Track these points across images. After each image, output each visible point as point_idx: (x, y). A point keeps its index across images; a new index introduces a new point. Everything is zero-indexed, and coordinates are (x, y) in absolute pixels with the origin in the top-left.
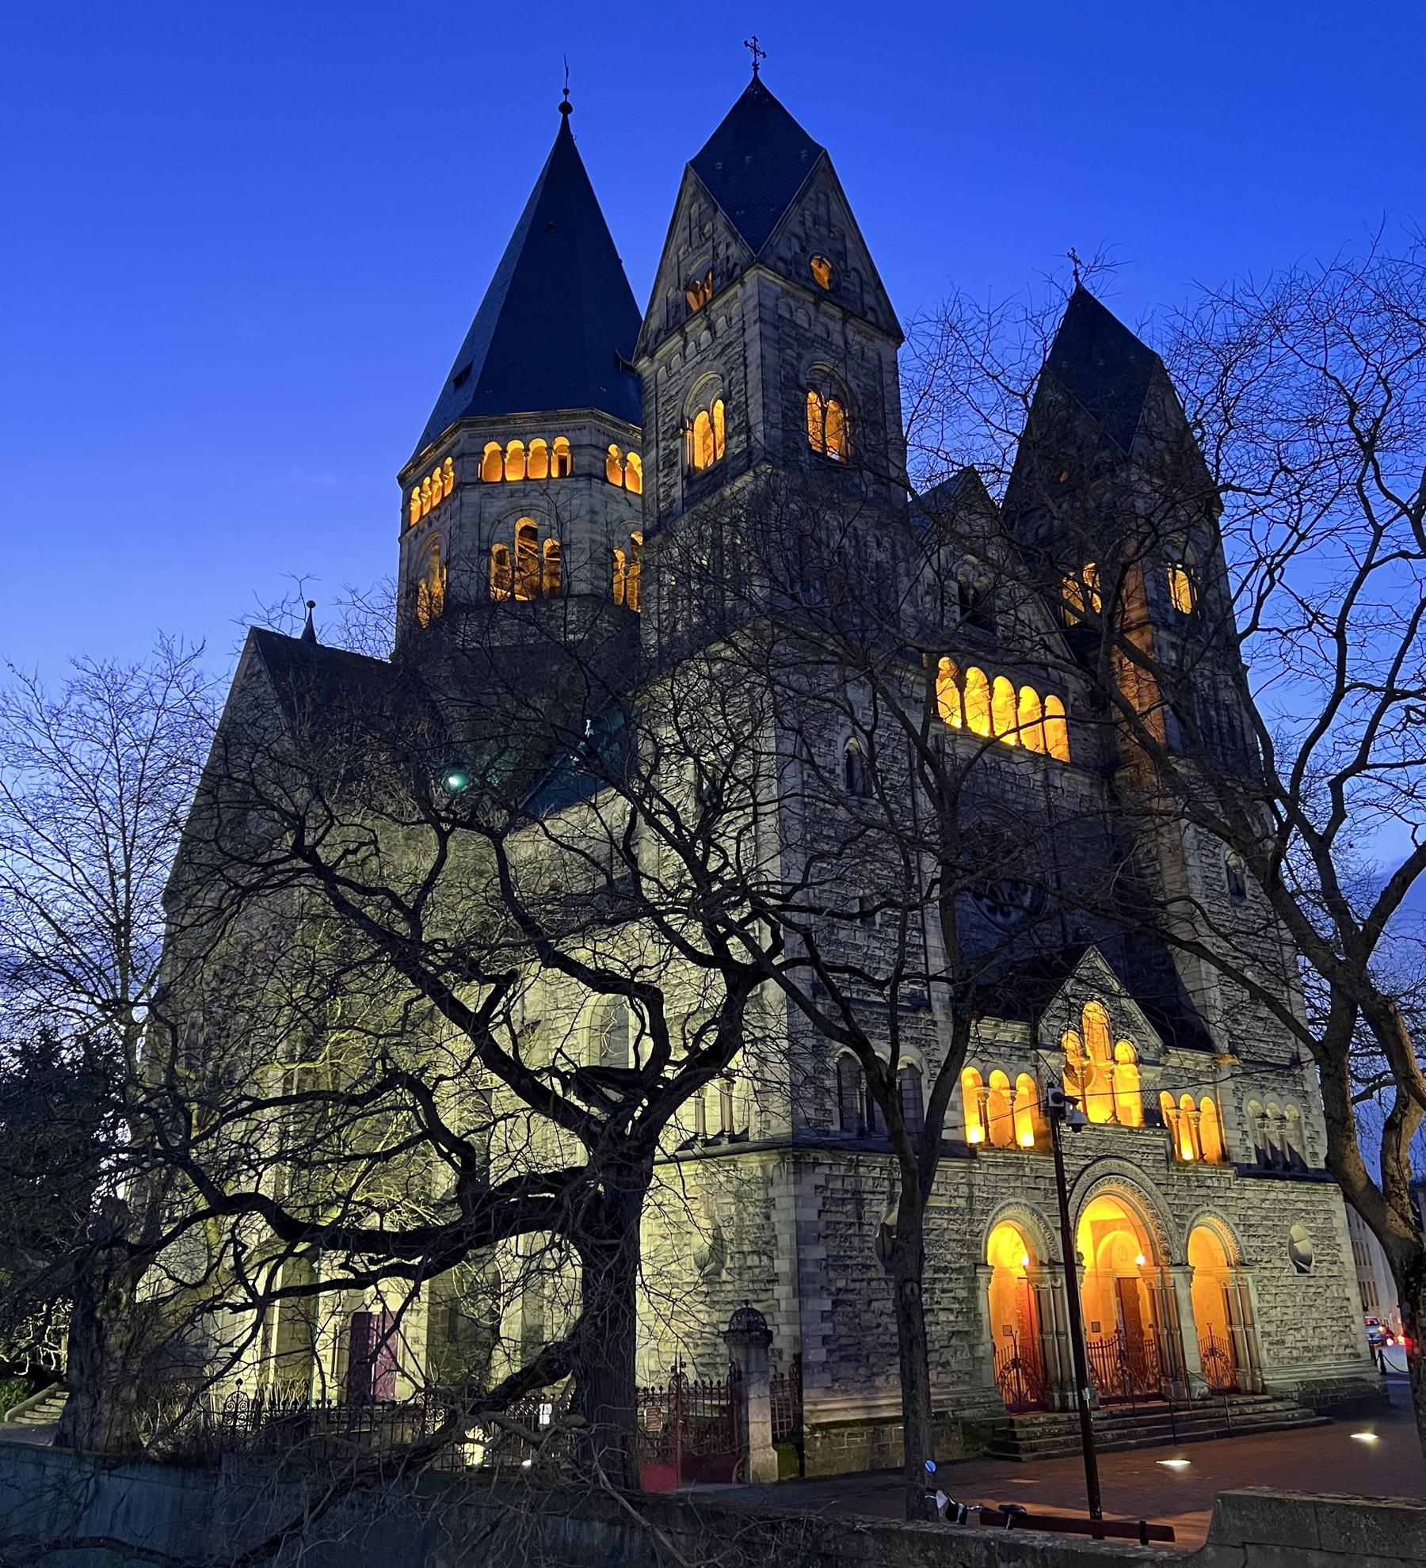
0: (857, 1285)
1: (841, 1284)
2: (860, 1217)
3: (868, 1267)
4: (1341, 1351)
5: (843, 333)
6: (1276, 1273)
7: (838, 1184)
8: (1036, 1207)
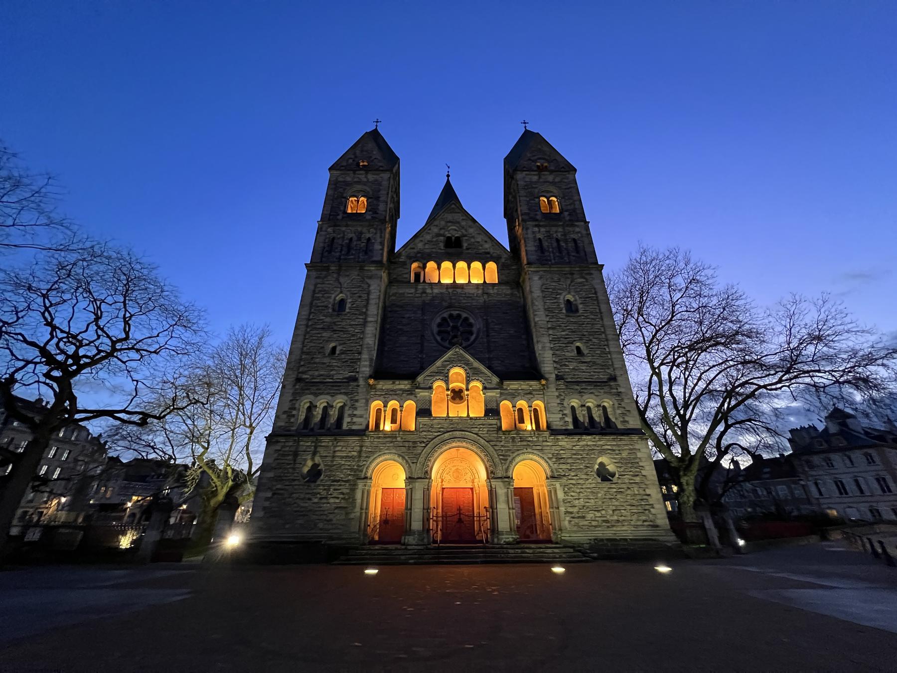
1: (279, 486)
2: (295, 461)
4: (640, 523)
6: (580, 481)
7: (287, 449)
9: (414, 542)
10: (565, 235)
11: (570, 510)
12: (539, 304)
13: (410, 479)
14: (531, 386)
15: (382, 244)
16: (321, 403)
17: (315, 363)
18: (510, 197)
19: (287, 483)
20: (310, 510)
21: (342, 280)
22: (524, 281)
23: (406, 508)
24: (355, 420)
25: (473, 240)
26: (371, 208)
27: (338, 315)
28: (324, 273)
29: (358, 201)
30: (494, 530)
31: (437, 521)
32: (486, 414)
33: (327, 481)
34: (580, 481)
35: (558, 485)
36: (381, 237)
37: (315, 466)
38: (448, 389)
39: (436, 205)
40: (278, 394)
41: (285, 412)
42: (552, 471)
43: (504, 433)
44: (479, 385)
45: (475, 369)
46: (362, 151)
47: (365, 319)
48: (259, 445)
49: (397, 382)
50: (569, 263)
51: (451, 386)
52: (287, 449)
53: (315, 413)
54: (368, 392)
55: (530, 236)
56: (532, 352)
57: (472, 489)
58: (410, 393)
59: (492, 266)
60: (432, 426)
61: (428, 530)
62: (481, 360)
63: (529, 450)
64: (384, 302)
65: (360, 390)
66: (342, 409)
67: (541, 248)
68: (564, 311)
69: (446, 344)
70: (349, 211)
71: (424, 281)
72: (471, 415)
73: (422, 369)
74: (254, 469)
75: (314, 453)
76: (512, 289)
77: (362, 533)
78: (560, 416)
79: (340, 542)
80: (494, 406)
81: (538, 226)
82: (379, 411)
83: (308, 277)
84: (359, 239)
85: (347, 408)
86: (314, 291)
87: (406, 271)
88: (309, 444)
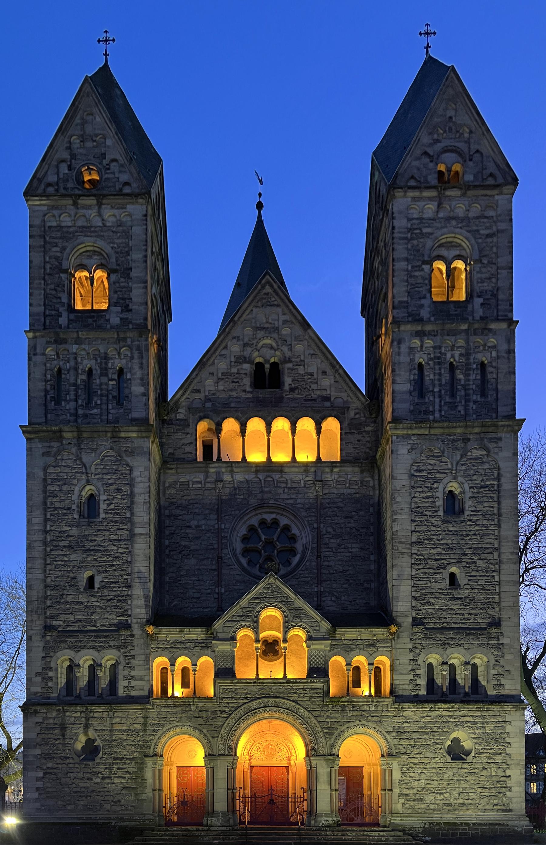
0: (60, 766)
1: (50, 765)
2: (63, 735)
5: (100, 215)
7: (51, 721)
8: (199, 727)
9: (219, 824)
10: (467, 355)
12: (403, 502)
13: (209, 756)
14: (375, 635)
15: (145, 383)
16: (85, 660)
17: (67, 603)
18: (376, 264)
19: (59, 761)
20: (93, 791)
21: (85, 458)
22: (383, 456)
23: (208, 789)
24: (133, 683)
26: (120, 298)
27: (89, 524)
28: (55, 444)
29: (92, 280)
30: (312, 812)
31: (244, 802)
32: (309, 675)
33: (107, 759)
36: (141, 368)
37: (90, 742)
38: (257, 641)
39: (238, 284)
40: (24, 647)
41: (38, 674)
42: (390, 748)
43: (332, 699)
44: (300, 633)
47: (131, 531)
48: (13, 714)
49: (186, 630)
50: (465, 417)
51: (262, 635)
52: (51, 721)
53: (79, 675)
54: (147, 645)
55: (404, 358)
57: (287, 767)
58: (205, 646)
59: (332, 425)
60: (235, 692)
61: (234, 812)
62: (305, 596)
63: (363, 722)
64: (159, 503)
65: (136, 642)
66: (114, 668)
67: (420, 386)
69: (256, 571)
70: (79, 306)
71: (219, 459)
72: (289, 676)
73: (221, 610)
74: (15, 745)
75: (86, 727)
76: (362, 472)
77: (156, 815)
79: (132, 823)
80: (320, 663)
81: (420, 334)
82: (164, 670)
83: (29, 450)
85: (120, 667)
86: (45, 480)
87: (188, 439)
88: (78, 715)
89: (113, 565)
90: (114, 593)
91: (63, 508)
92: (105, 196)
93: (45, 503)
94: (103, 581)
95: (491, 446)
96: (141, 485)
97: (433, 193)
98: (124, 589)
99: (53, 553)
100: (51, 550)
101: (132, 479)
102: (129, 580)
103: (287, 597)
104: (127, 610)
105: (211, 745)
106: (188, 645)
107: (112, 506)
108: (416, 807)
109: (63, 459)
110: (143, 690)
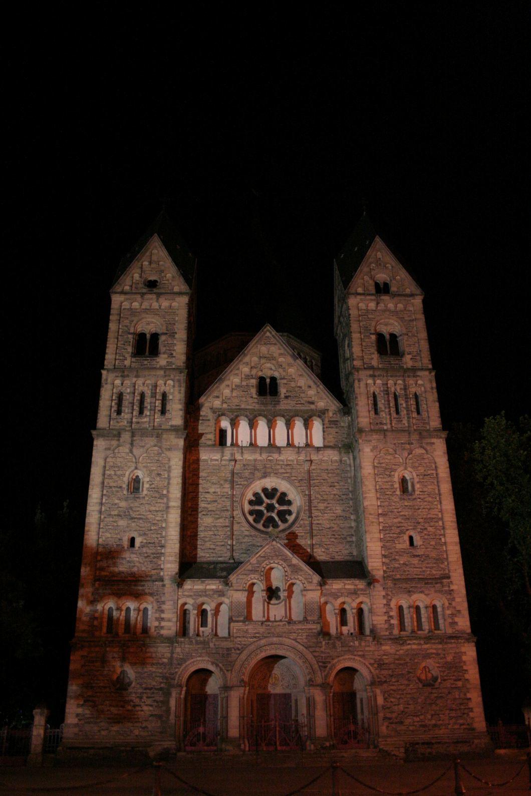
0: (98, 694)
1: (90, 694)
3: (105, 687)
6: (402, 687)
11: (388, 715)
24: (163, 624)
25: (293, 384)
27: (136, 498)
28: (114, 443)
34: (402, 687)
35: (378, 691)
45: (294, 565)
46: (150, 263)
47: (167, 503)
56: (360, 544)
65: (166, 590)
68: (398, 492)
78: (386, 618)
81: (373, 376)
84: (154, 395)
86: (105, 467)
89: (151, 530)
90: (151, 551)
91: (117, 487)
92: (162, 294)
93: (103, 483)
94: (142, 542)
95: (428, 448)
96: (176, 471)
97: (373, 297)
98: (159, 548)
99: (106, 519)
100: (105, 518)
101: (169, 467)
102: (163, 542)
103: (286, 556)
104: (160, 565)
105: (226, 677)
106: (207, 593)
107: (153, 486)
108: (398, 729)
109: (119, 452)
110: (170, 629)
